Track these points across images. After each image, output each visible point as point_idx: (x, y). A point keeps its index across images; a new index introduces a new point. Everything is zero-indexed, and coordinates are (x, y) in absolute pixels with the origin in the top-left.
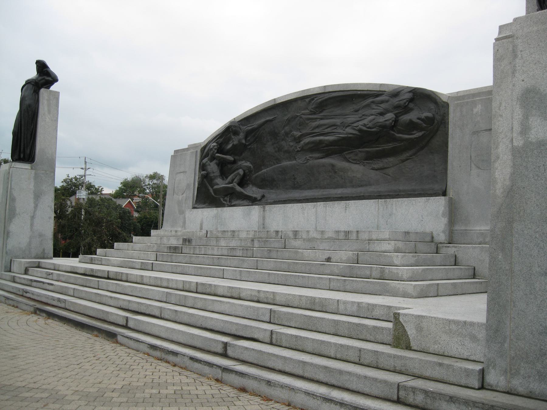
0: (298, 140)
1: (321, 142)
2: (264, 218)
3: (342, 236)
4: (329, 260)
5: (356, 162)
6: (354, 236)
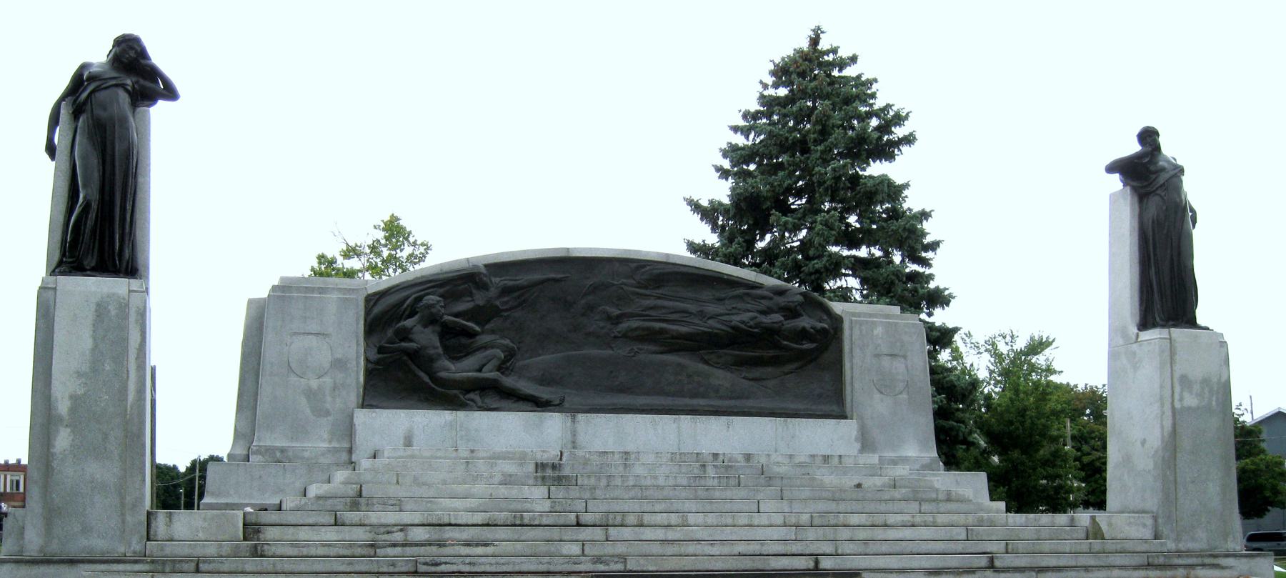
0: (617, 320)
1: (662, 331)
2: (574, 433)
3: (819, 460)
4: (859, 486)
5: (725, 367)
6: (836, 460)
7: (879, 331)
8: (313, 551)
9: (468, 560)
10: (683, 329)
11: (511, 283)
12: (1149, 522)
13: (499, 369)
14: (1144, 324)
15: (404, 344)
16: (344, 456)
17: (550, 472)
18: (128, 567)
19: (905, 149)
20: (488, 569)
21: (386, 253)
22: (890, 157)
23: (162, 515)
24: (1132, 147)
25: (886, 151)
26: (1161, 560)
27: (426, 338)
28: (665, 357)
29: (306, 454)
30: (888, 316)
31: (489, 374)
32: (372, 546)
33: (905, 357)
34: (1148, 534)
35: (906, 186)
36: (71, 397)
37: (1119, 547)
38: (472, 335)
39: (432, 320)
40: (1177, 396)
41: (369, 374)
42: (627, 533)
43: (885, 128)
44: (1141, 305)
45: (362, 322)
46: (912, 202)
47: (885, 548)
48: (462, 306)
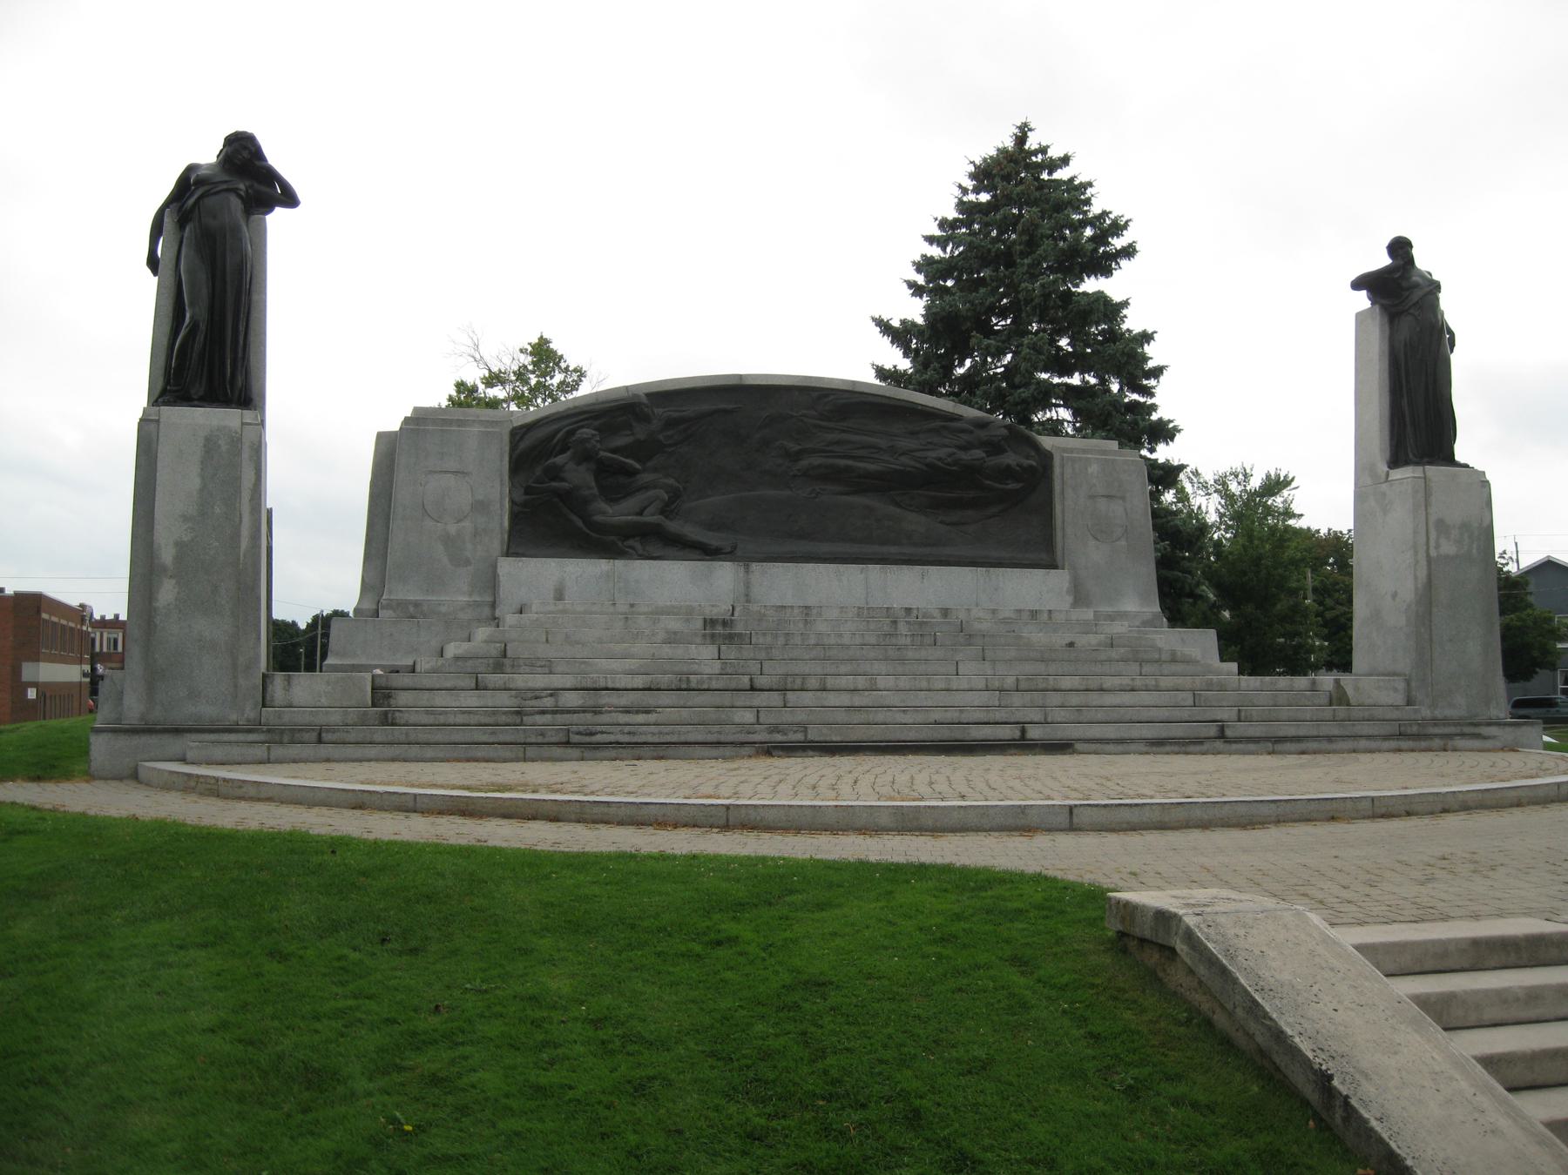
0: (796, 456)
1: (848, 469)
2: (748, 585)
4: (1071, 645)
7: (1093, 469)
8: (451, 720)
9: (627, 729)
10: (872, 467)
11: (676, 415)
12: (1401, 685)
13: (662, 512)
14: (1396, 461)
15: (554, 484)
16: (487, 611)
17: (720, 630)
18: (241, 737)
19: (1124, 263)
20: (650, 739)
21: (533, 380)
22: (1107, 272)
23: (279, 677)
24: (1383, 261)
25: (1103, 265)
26: (1415, 729)
27: (579, 476)
29: (443, 609)
30: (1104, 452)
31: (650, 517)
32: (518, 713)
33: (1123, 498)
34: (1399, 699)
35: (1125, 304)
36: (177, 544)
37: (1366, 714)
38: (631, 473)
39: (585, 456)
40: (1432, 543)
41: (515, 517)
42: (807, 698)
43: (1102, 237)
44: (1391, 439)
45: (507, 459)
46: (1133, 322)
47: (1100, 716)
48: (621, 441)
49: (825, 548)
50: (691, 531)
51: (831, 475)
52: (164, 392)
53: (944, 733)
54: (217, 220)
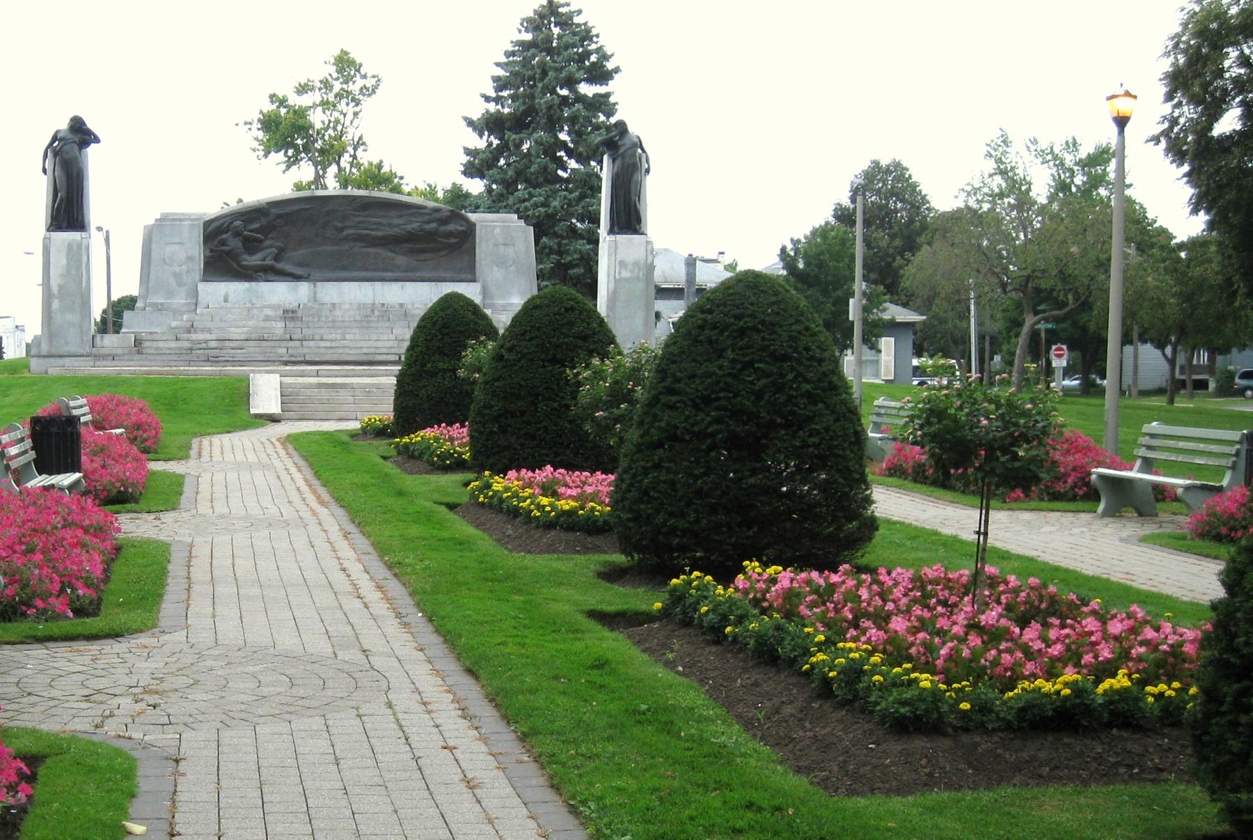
1: (367, 235)
2: (315, 293)
5: (403, 254)
7: (497, 230)
10: (380, 234)
17: (290, 315)
21: (337, 87)
23: (99, 336)
27: (235, 244)
28: (370, 250)
31: (268, 262)
38: (260, 241)
39: (237, 234)
41: (207, 264)
42: (312, 343)
49: (355, 274)
50: (289, 268)
51: (359, 238)
52: (51, 225)
53: (365, 358)
54: (70, 151)
